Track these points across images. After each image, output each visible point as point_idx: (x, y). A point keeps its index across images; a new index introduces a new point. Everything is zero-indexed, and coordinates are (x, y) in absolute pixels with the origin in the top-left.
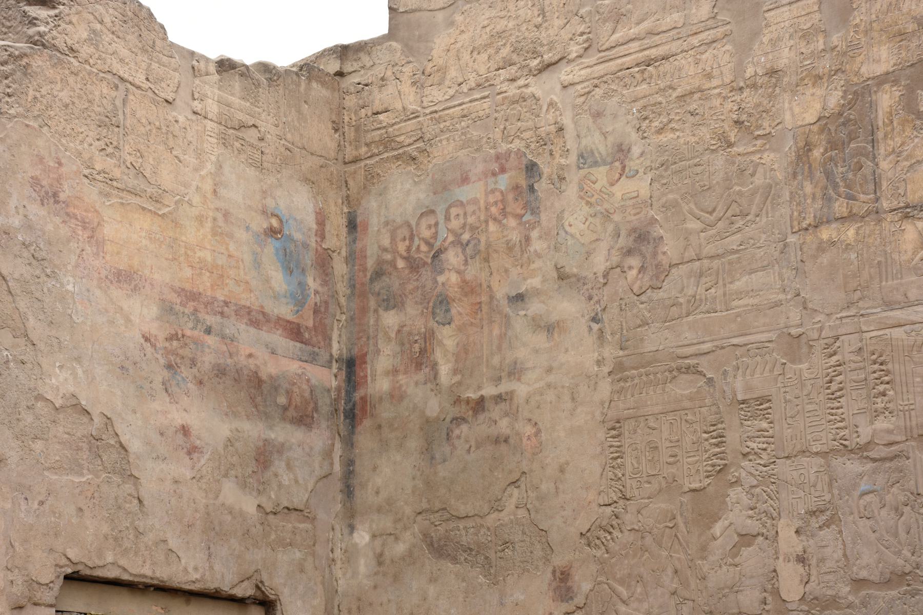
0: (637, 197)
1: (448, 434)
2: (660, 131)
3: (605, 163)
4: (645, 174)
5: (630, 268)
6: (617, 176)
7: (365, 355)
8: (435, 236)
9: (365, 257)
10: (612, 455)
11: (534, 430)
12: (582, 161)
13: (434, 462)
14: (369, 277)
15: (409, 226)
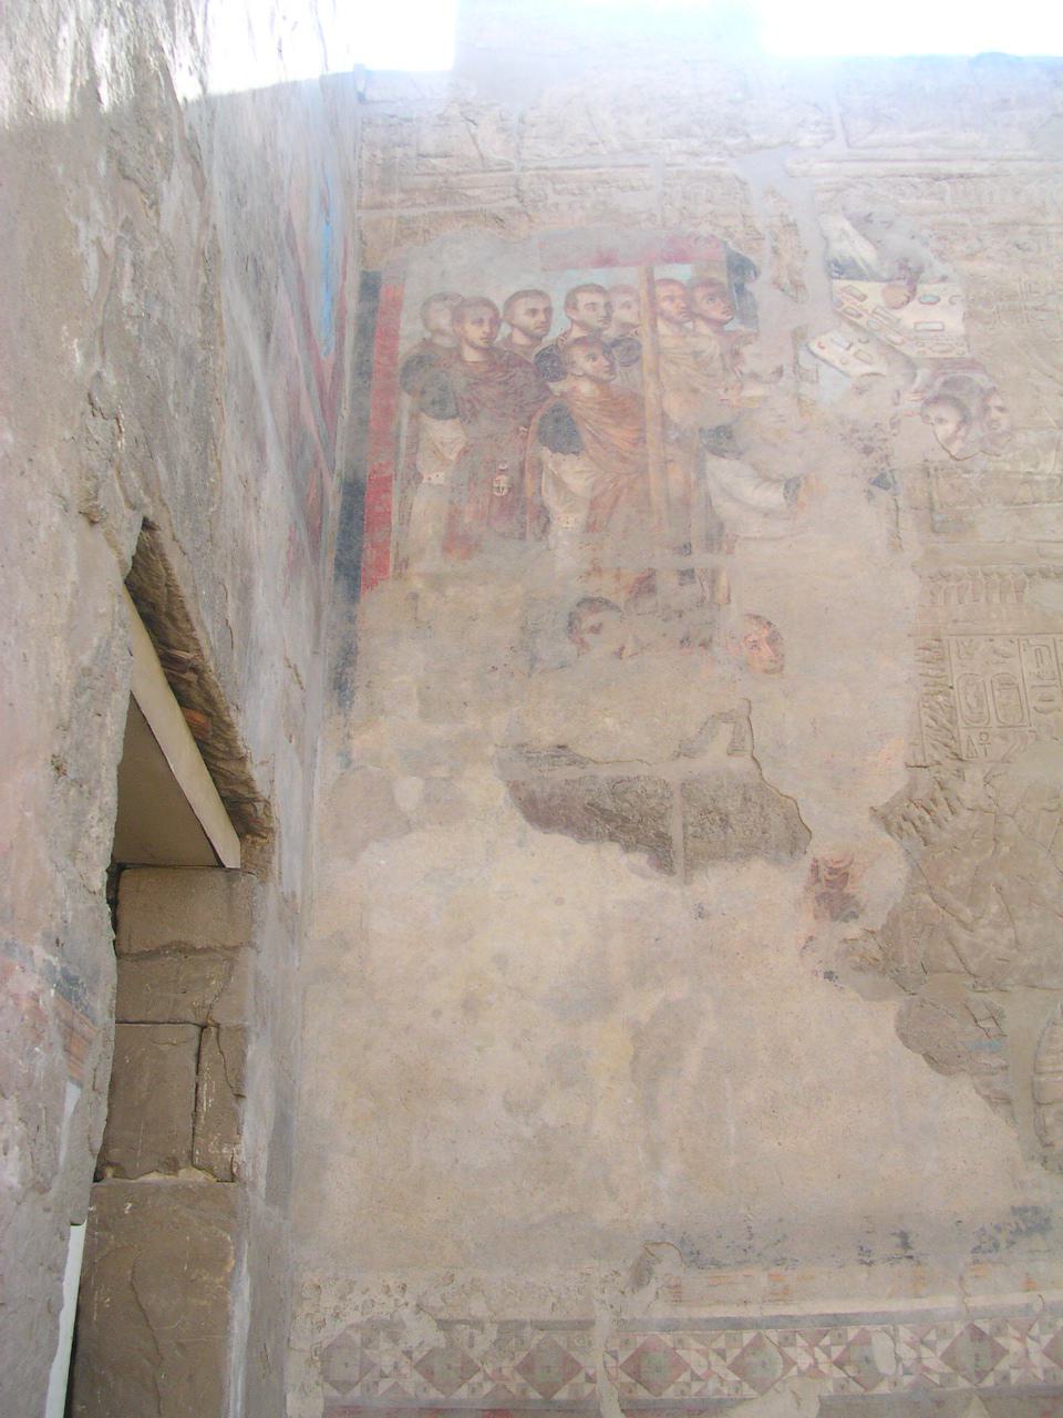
0: (943, 330)
1: (570, 624)
2: (971, 256)
3: (875, 278)
4: (952, 303)
5: (941, 421)
6: (905, 298)
7: (389, 479)
8: (546, 326)
9: (396, 337)
10: (925, 690)
11: (766, 633)
12: (837, 269)
13: (538, 666)
14: (400, 366)
15: (488, 303)
